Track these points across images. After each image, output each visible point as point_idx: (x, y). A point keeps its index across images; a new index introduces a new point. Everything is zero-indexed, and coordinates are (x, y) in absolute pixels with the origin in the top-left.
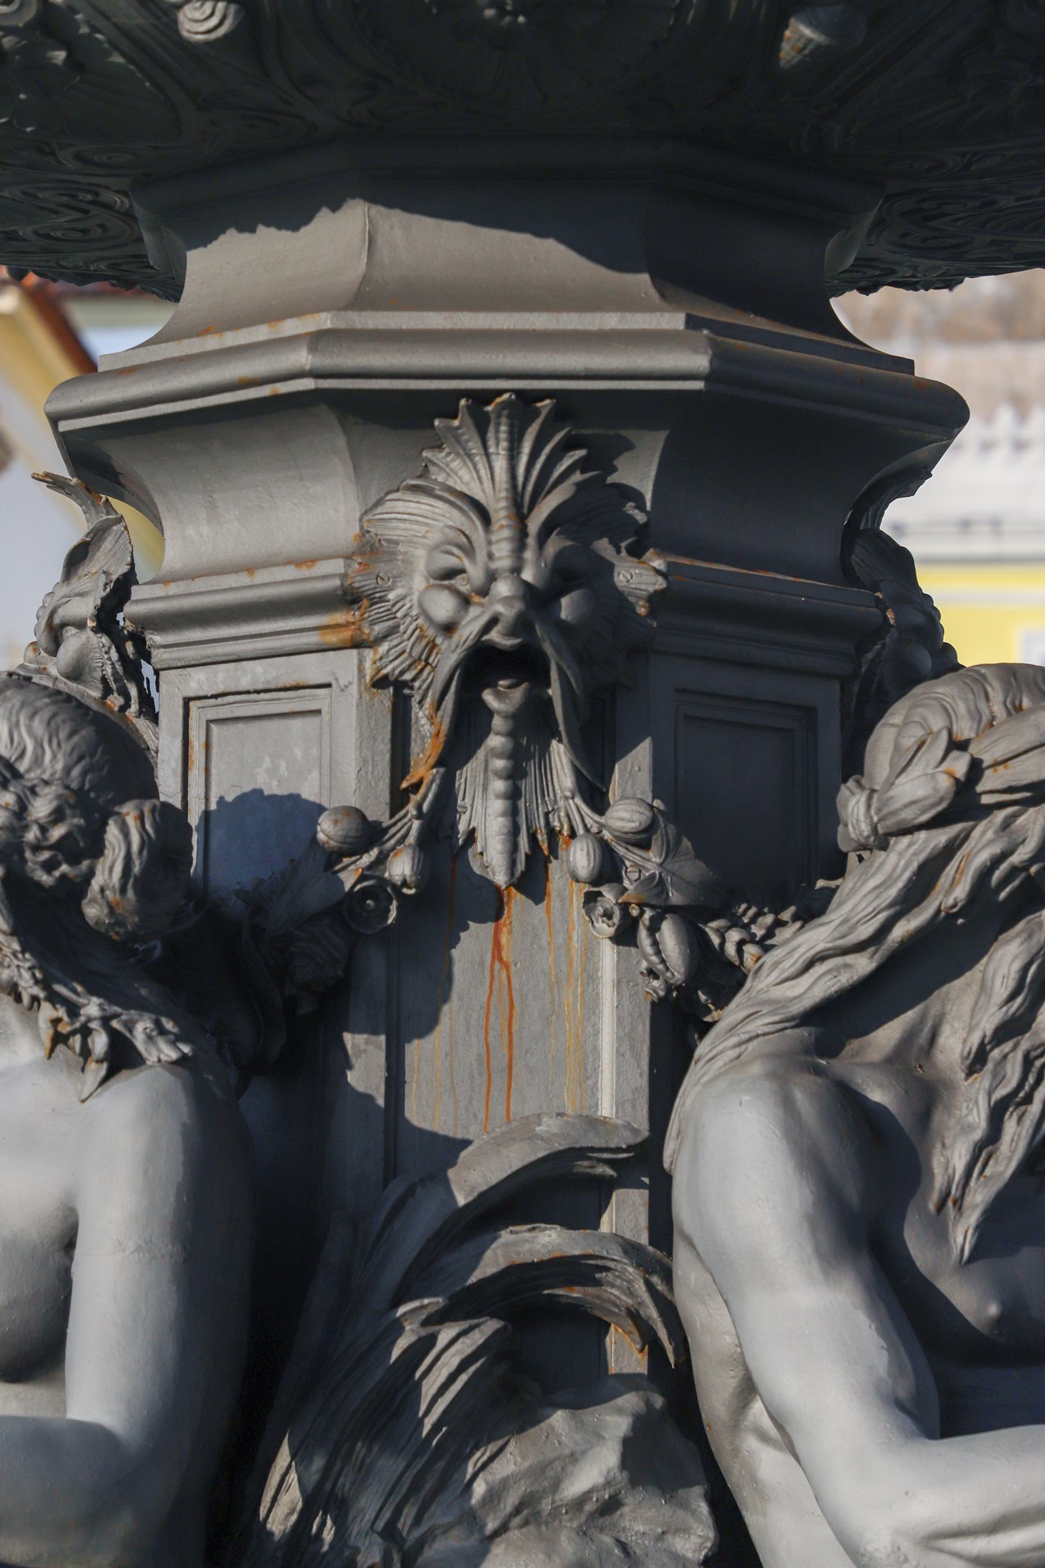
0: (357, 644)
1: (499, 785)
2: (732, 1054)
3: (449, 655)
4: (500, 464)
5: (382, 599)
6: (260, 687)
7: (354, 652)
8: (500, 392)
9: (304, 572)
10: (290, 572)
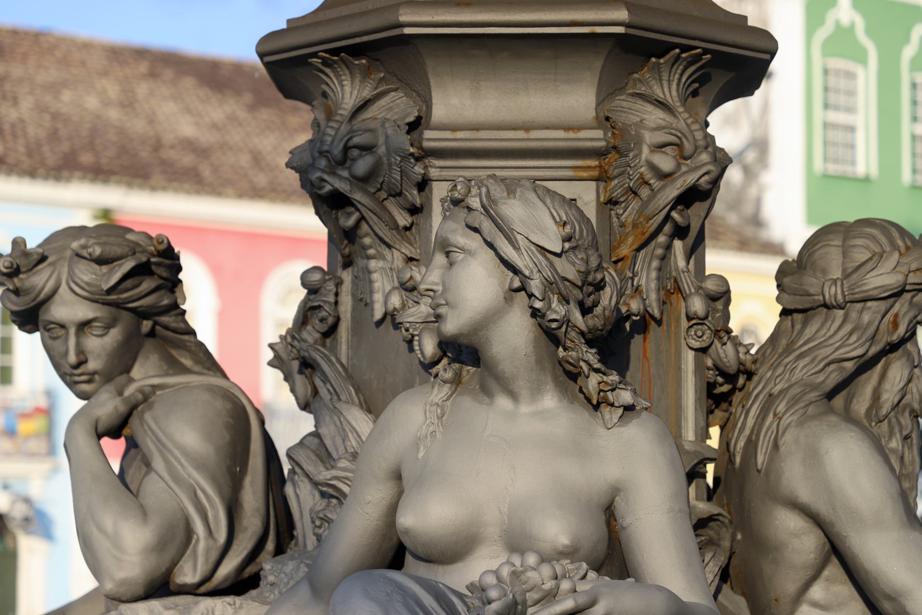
0: (597, 179)
1: (655, 264)
2: (801, 412)
3: (673, 191)
4: (674, 86)
5: (626, 156)
7: (594, 184)
8: (696, 48)
9: (571, 135)
10: (560, 134)
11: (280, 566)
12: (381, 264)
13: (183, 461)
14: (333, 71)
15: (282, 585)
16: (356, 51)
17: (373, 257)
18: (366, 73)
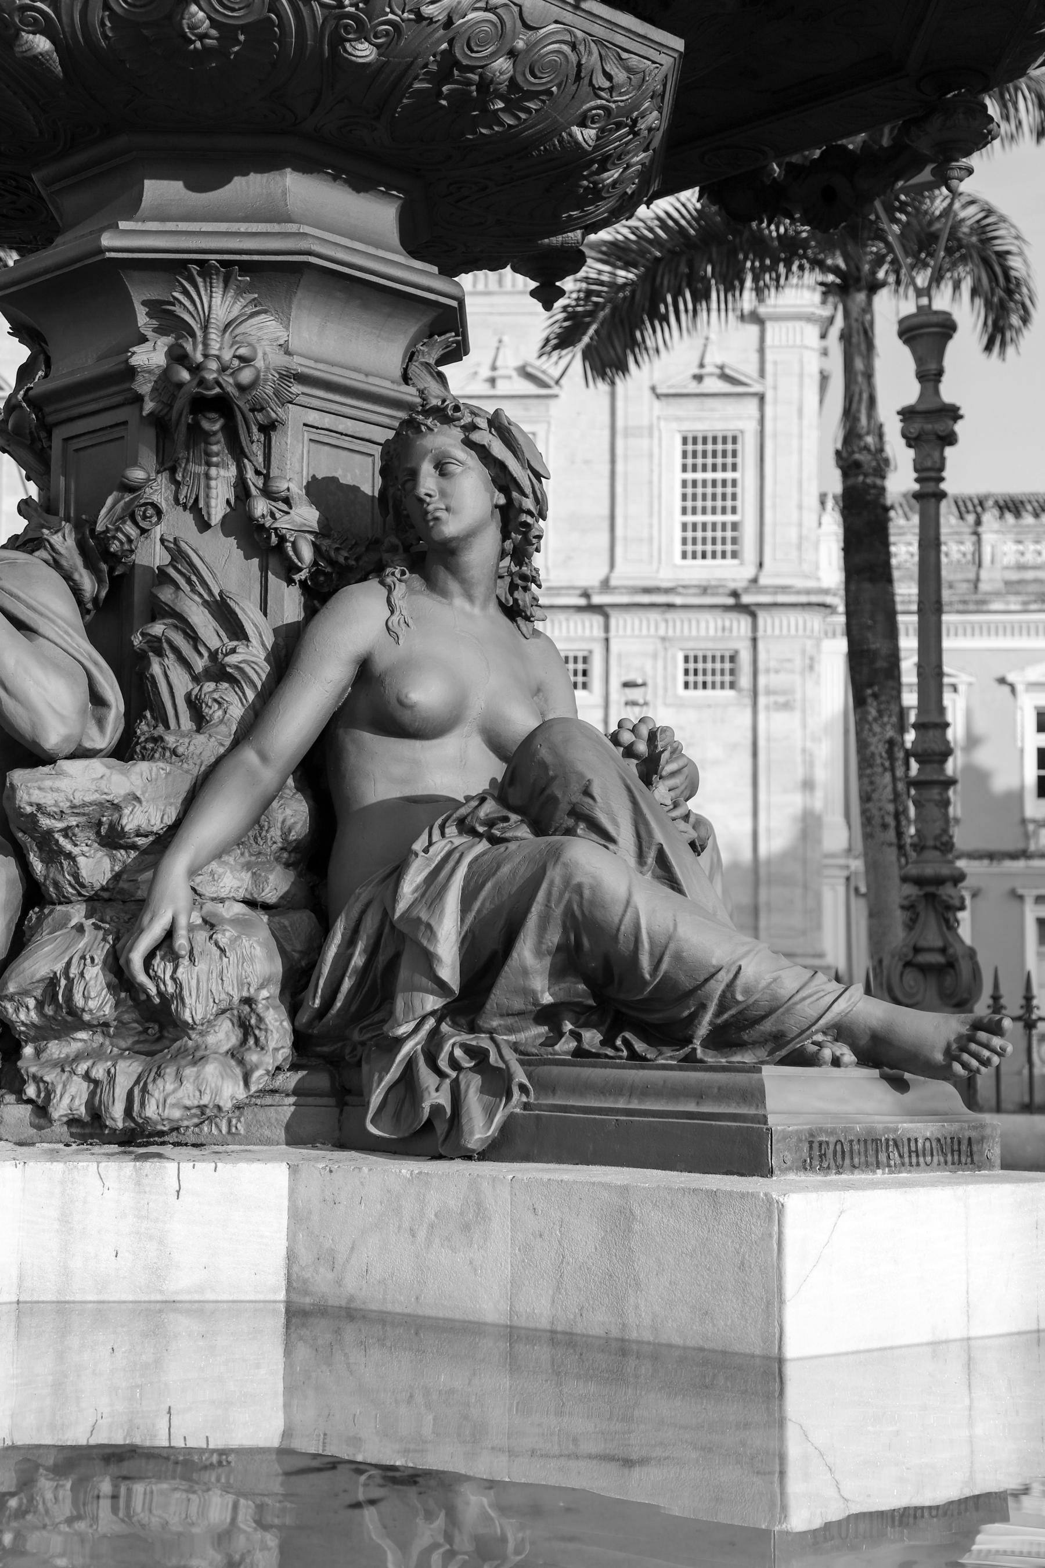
6: (349, 433)
11: (187, 740)
12: (222, 472)
13: (71, 631)
14: (205, 282)
15: (195, 757)
16: (246, 268)
17: (217, 465)
18: (240, 292)
